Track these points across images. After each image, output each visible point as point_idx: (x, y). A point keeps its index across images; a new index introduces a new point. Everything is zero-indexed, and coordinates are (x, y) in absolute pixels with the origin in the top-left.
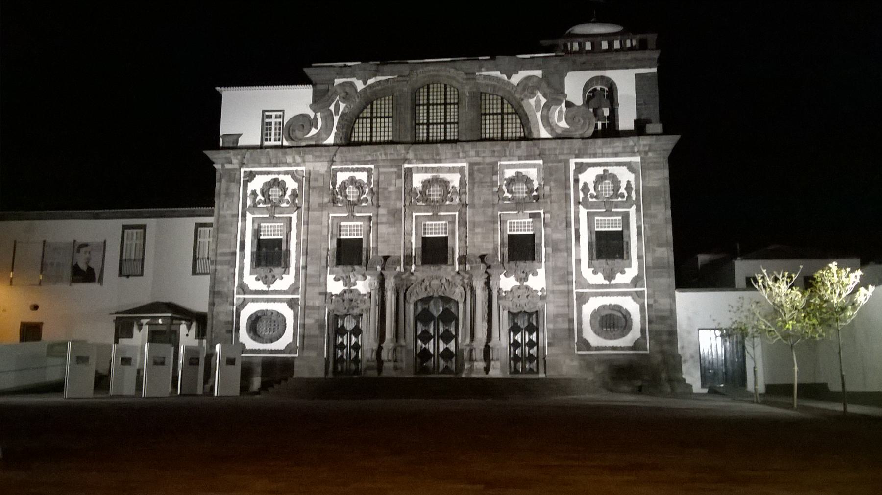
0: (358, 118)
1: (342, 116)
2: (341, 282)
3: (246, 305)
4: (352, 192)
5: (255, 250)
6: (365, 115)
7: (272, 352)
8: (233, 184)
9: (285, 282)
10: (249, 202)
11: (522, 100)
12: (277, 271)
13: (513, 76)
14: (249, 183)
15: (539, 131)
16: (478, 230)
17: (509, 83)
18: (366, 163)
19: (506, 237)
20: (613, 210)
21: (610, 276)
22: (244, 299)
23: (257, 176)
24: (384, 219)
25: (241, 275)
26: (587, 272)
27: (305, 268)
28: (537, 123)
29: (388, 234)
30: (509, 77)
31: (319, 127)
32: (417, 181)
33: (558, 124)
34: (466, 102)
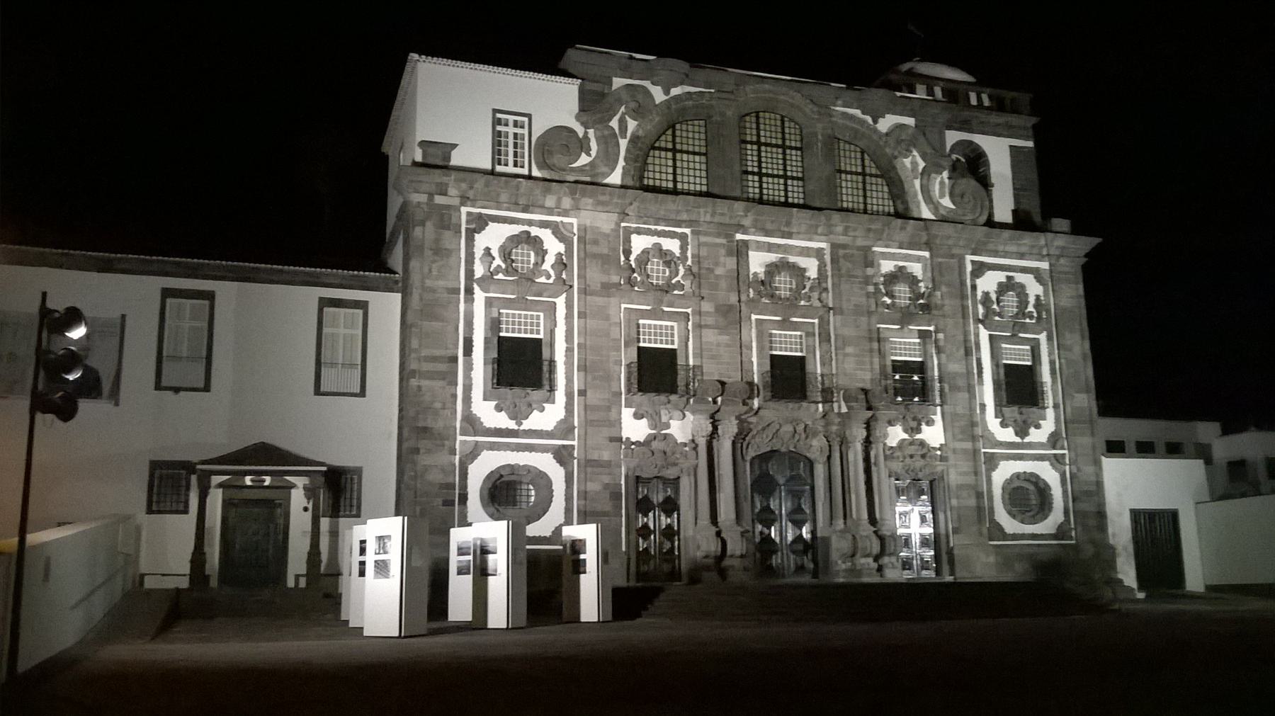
0: (654, 148)
1: (635, 140)
2: (644, 421)
4: (657, 271)
6: (663, 145)
8: (447, 234)
9: (547, 417)
10: (479, 271)
11: (896, 158)
12: (535, 395)
13: (881, 120)
15: (918, 206)
16: (849, 350)
17: (876, 131)
18: (678, 224)
19: (889, 363)
20: (1022, 335)
21: (1022, 431)
23: (490, 223)
24: (710, 320)
25: (467, 400)
26: (993, 423)
27: (582, 393)
28: (916, 195)
29: (718, 345)
30: (875, 122)
31: (593, 153)
32: (757, 262)
33: (940, 201)
34: (817, 148)
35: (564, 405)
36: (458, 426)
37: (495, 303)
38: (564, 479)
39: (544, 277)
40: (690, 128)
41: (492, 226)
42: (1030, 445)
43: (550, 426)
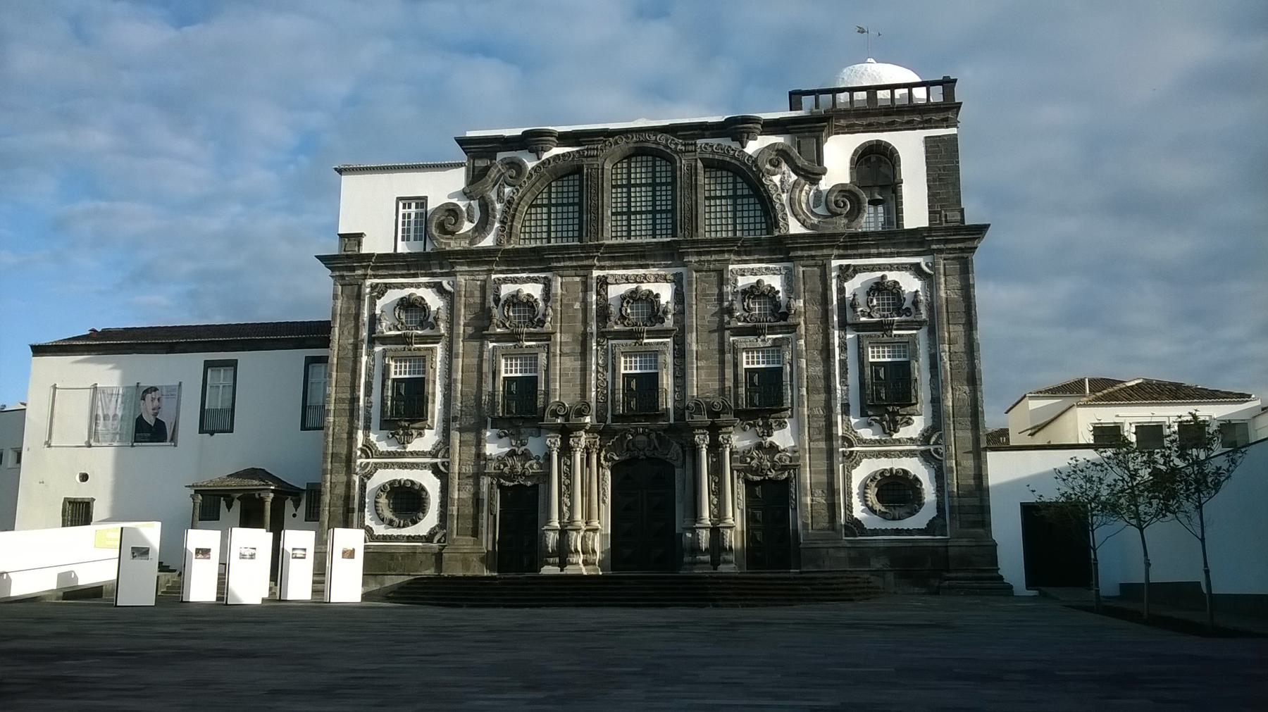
7: (410, 538)
9: (427, 440)
30: (743, 147)
33: (813, 210)
40: (565, 183)
42: (899, 441)
43: (428, 448)
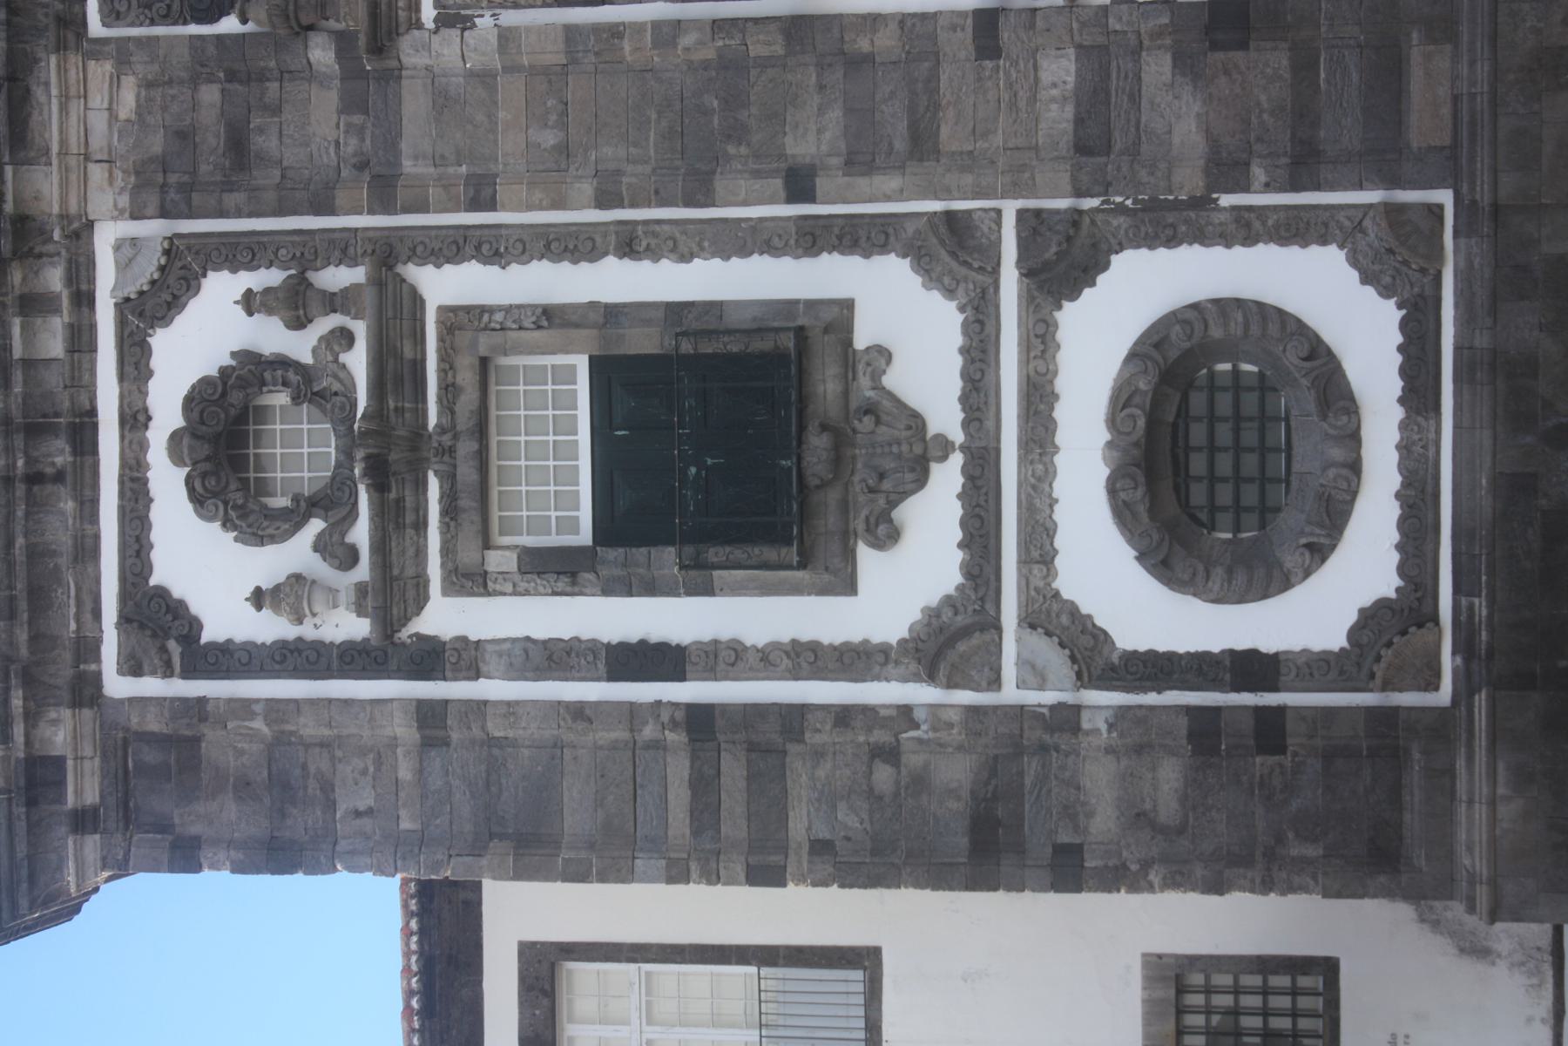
3: (1073, 610)
5: (667, 558)
8: (216, 745)
12: (826, 385)
14: (206, 636)
22: (1030, 621)
27: (799, 186)
35: (854, 263)
36: (965, 697)
37: (468, 554)
38: (1162, 252)
39: (344, 358)
41: (168, 571)
